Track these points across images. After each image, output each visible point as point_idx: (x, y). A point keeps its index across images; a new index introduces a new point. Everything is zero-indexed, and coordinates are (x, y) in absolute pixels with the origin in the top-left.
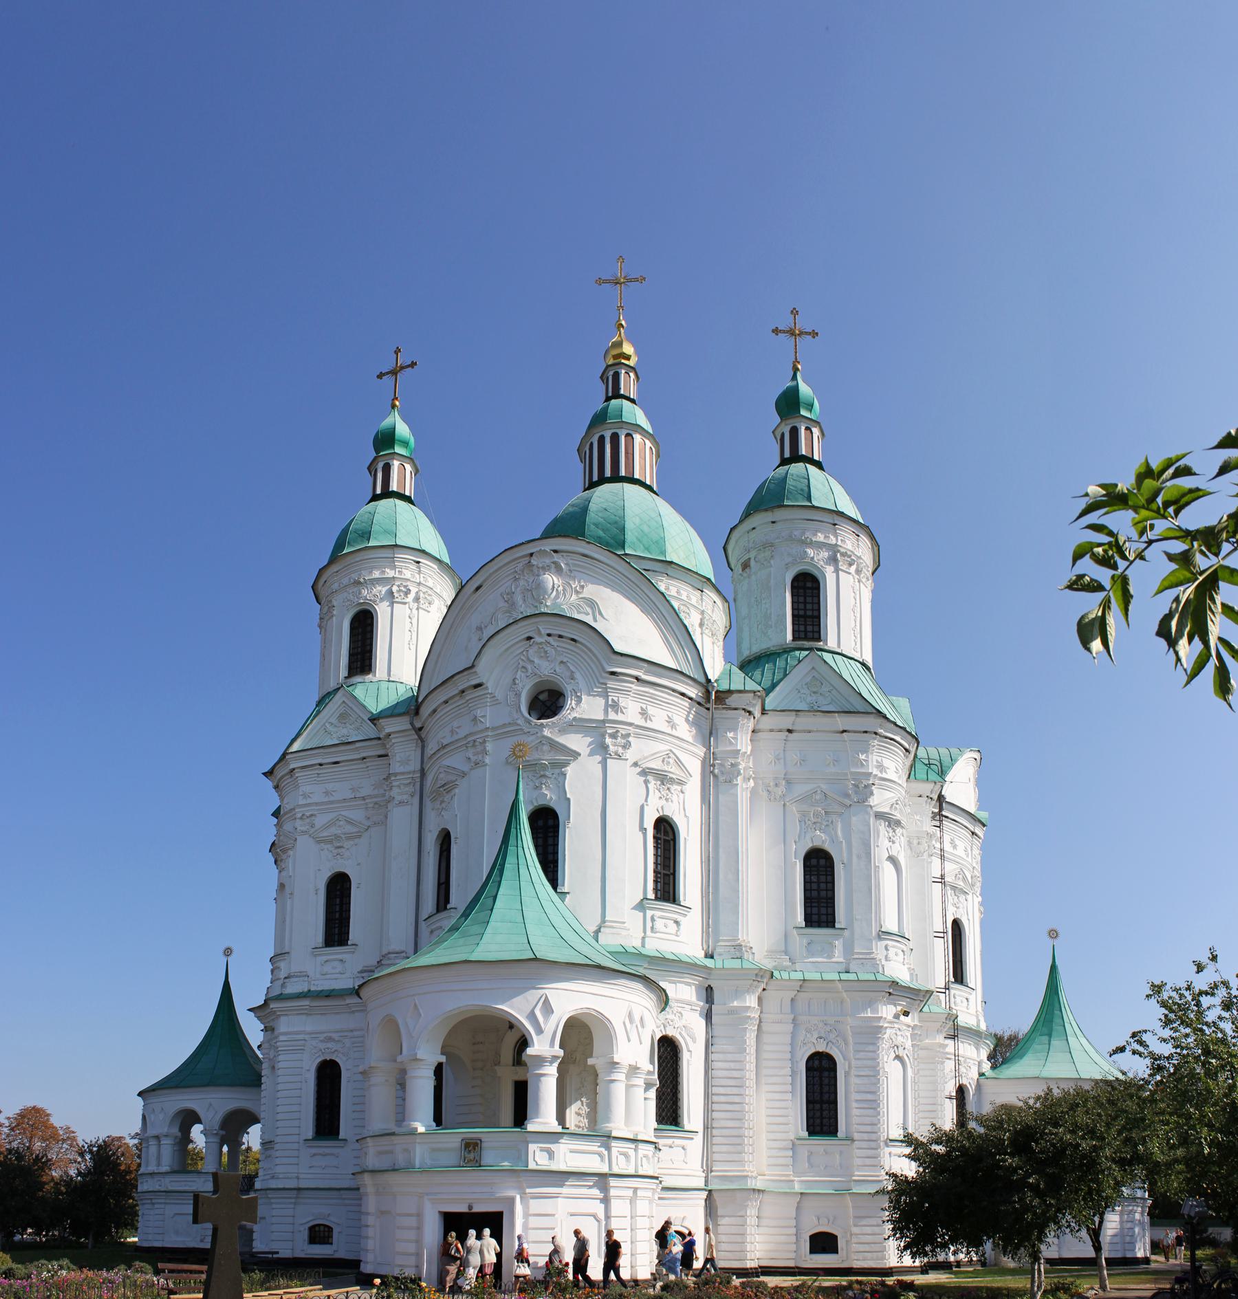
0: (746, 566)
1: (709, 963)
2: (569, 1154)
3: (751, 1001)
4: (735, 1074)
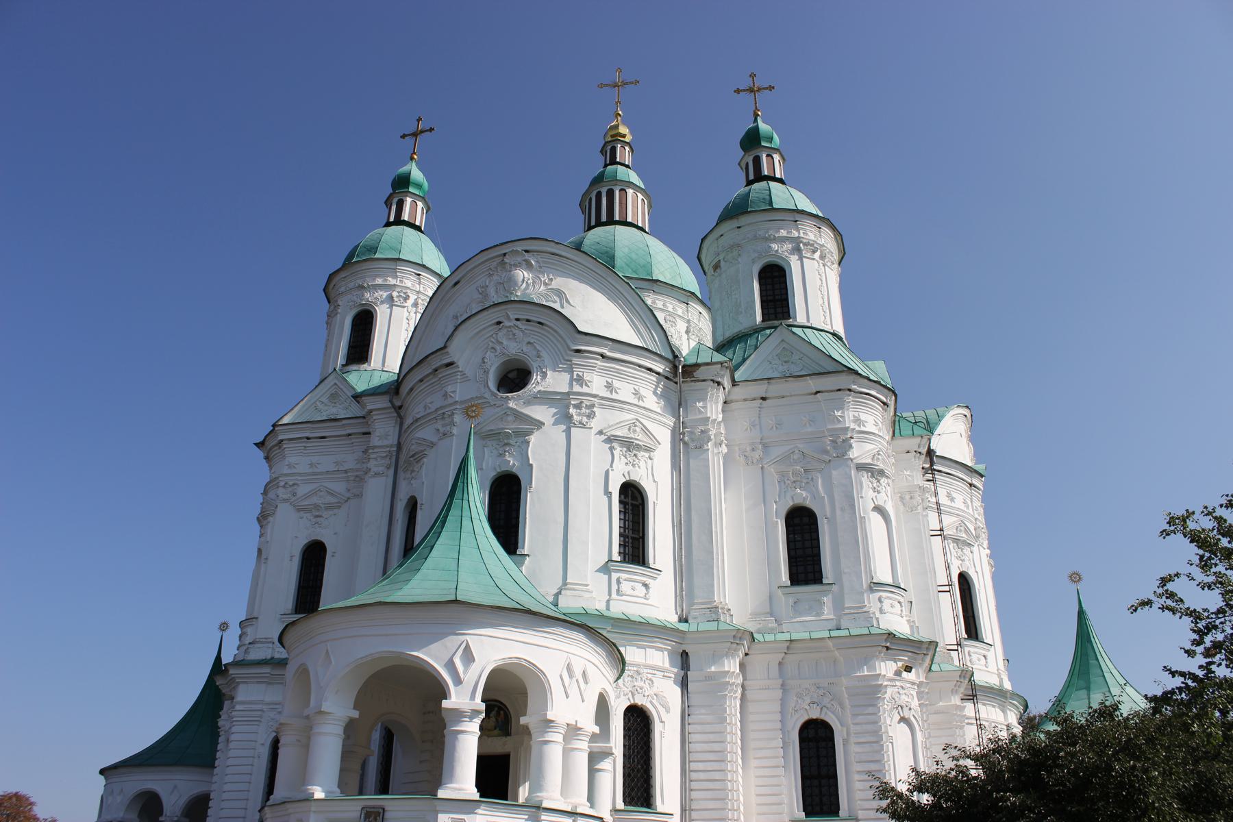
0: (717, 267)
1: (683, 627)
3: (732, 665)
4: (716, 747)
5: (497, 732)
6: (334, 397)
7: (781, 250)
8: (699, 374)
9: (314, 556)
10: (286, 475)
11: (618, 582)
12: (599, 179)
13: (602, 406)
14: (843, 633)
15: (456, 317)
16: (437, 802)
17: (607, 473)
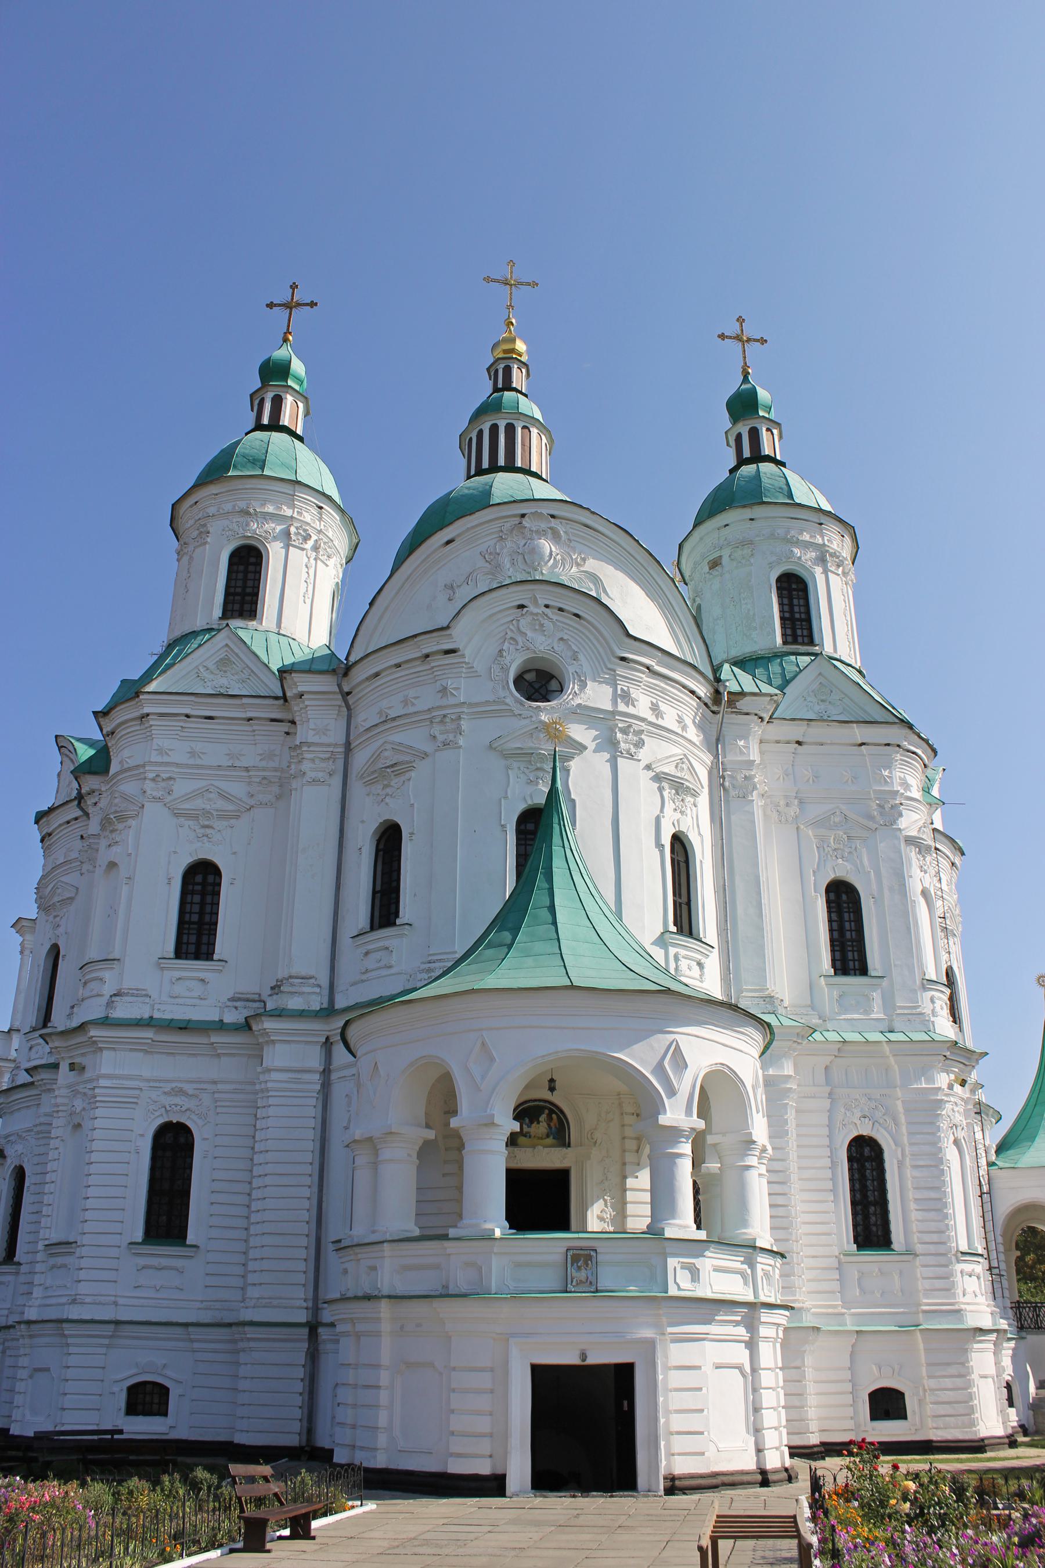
2: (712, 1273)
5: (550, 1141)
6: (224, 663)
7: (804, 559)
8: (743, 704)
9: (201, 882)
10: (157, 764)
11: (676, 958)
12: (489, 408)
13: (651, 734)
14: (901, 1037)
15: (451, 587)
16: (667, 1243)
17: (658, 820)
